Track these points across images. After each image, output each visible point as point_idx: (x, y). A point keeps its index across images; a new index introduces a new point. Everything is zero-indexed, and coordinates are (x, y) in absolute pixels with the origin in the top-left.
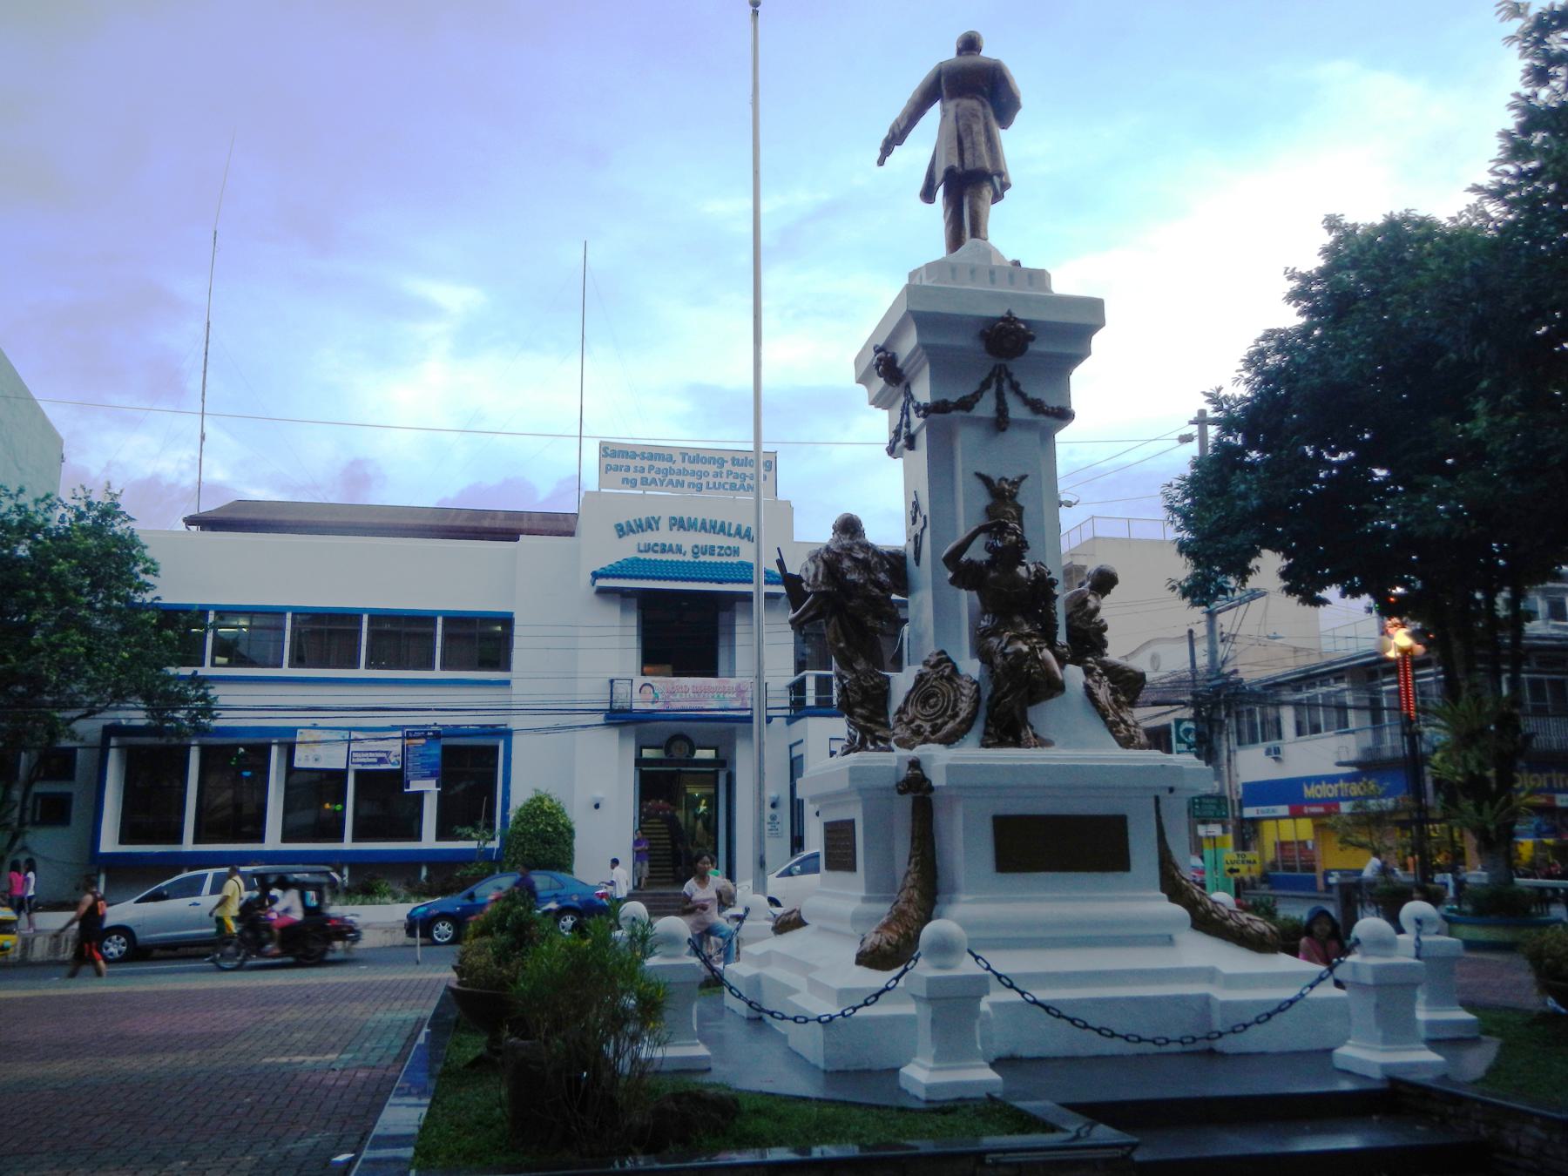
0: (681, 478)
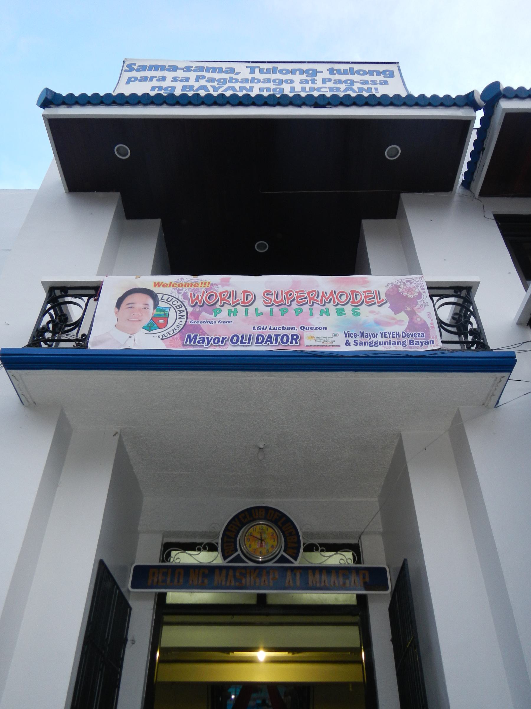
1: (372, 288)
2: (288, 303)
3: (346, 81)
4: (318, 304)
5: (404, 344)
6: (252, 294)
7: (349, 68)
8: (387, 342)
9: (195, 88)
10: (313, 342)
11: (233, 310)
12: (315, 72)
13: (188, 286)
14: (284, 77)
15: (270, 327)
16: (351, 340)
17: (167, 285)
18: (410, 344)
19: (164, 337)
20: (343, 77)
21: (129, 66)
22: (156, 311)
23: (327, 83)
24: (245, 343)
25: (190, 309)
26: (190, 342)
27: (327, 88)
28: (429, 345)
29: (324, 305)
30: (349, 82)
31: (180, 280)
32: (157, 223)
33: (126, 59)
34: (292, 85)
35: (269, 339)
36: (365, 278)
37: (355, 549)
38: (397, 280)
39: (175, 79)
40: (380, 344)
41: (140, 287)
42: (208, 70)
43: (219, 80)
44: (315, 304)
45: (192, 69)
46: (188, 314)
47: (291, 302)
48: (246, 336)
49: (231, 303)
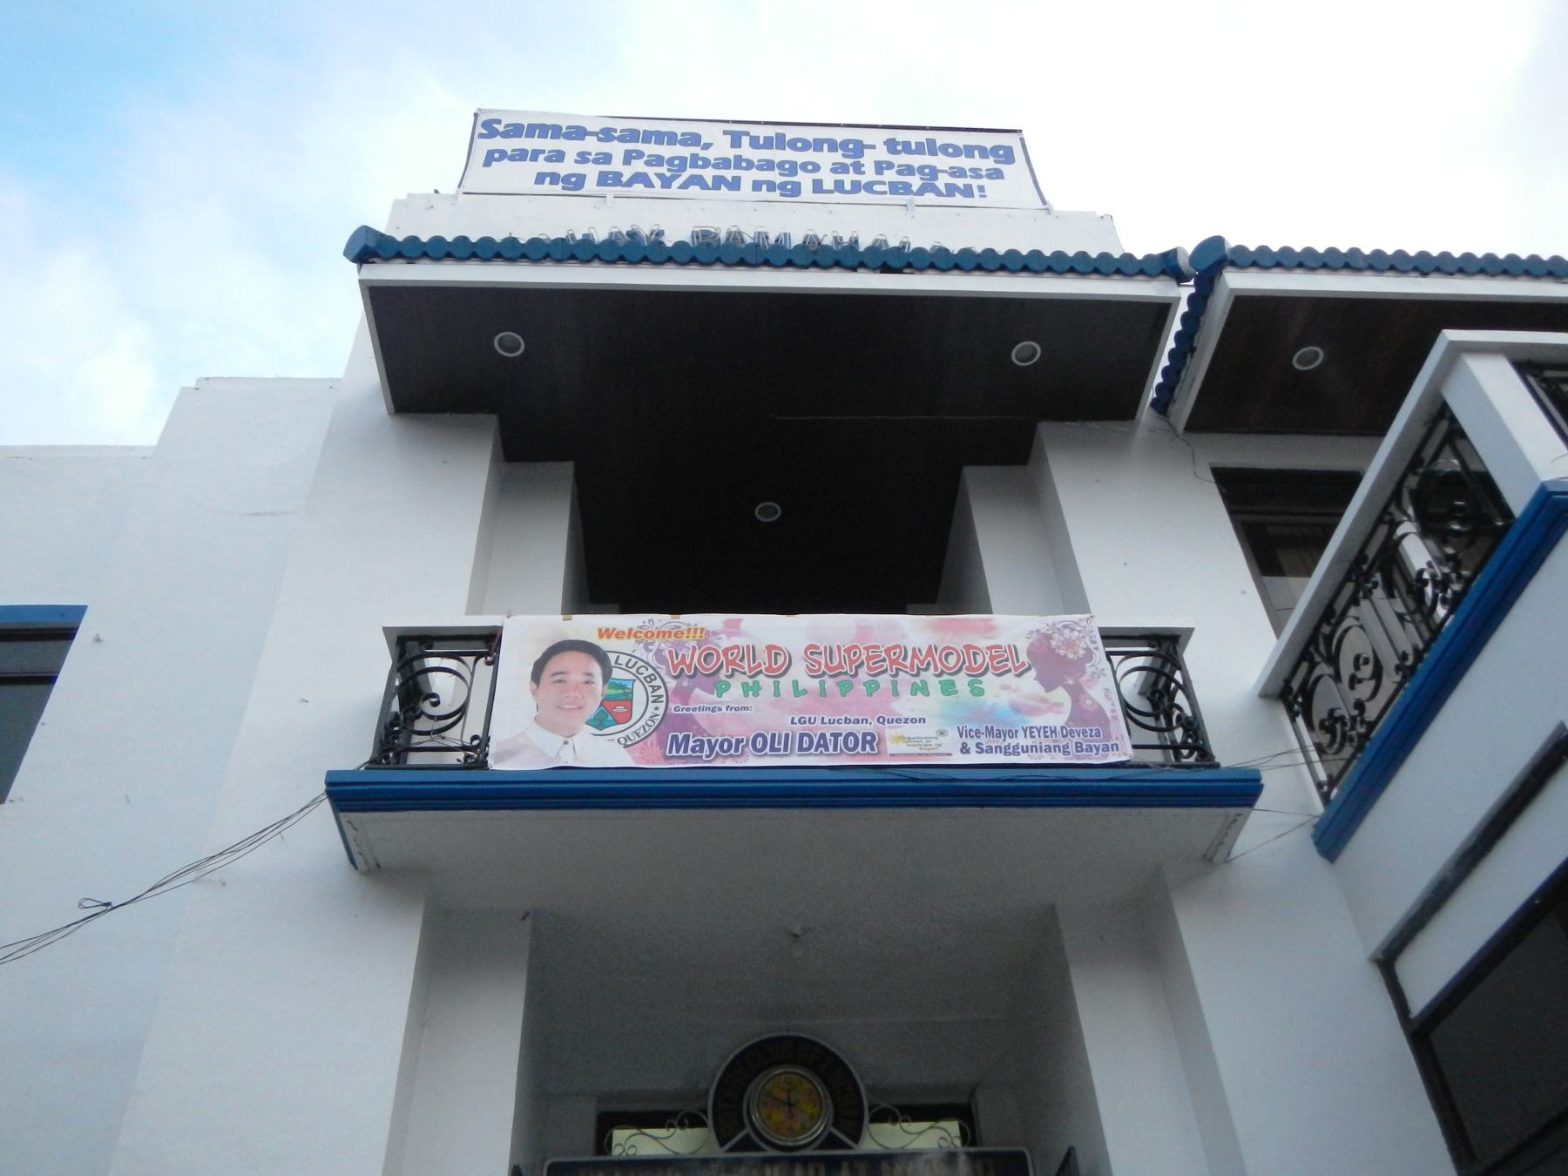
0: (729, 174)
1: (1003, 640)
2: (851, 670)
3: (921, 169)
4: (907, 672)
5: (1066, 753)
6: (783, 652)
7: (927, 140)
8: (1036, 747)
9: (624, 179)
10: (902, 748)
11: (751, 685)
12: (859, 148)
13: (664, 636)
14: (800, 157)
15: (823, 718)
16: (971, 743)
17: (623, 633)
18: (1077, 751)
19: (629, 743)
20: (916, 161)
21: (488, 124)
22: (609, 688)
23: (885, 172)
24: (779, 750)
25: (671, 684)
26: (678, 751)
27: (884, 183)
28: (1110, 753)
29: (917, 675)
30: (927, 171)
31: (647, 624)
32: (568, 468)
33: (479, 110)
34: (817, 176)
35: (822, 742)
36: (990, 620)
37: (964, 1113)
38: (1048, 625)
39: (583, 158)
40: (1023, 752)
41: (573, 637)
42: (648, 137)
43: (670, 161)
44: (900, 673)
45: (616, 135)
46: (669, 693)
47: (857, 668)
48: (780, 736)
49: (746, 669)
